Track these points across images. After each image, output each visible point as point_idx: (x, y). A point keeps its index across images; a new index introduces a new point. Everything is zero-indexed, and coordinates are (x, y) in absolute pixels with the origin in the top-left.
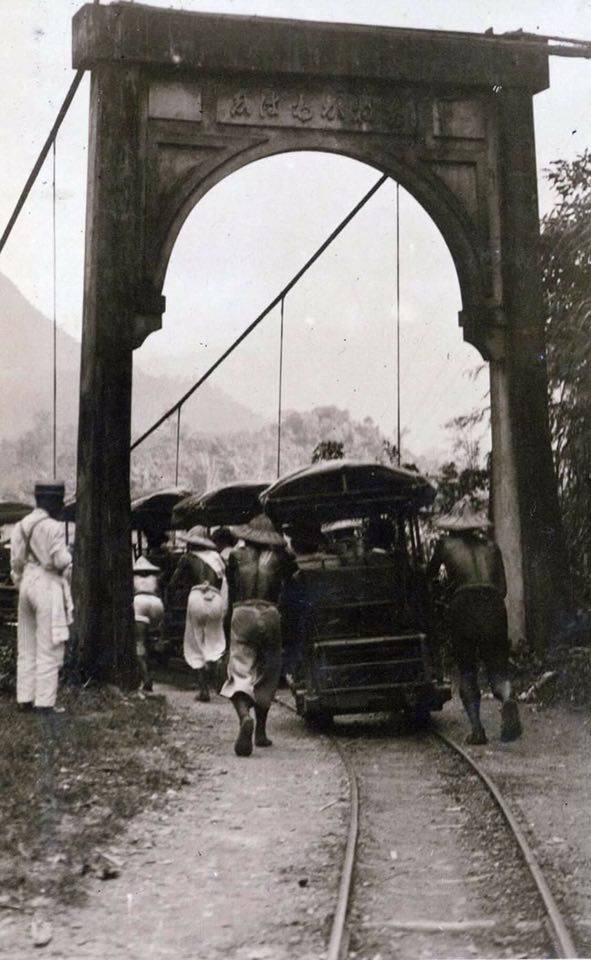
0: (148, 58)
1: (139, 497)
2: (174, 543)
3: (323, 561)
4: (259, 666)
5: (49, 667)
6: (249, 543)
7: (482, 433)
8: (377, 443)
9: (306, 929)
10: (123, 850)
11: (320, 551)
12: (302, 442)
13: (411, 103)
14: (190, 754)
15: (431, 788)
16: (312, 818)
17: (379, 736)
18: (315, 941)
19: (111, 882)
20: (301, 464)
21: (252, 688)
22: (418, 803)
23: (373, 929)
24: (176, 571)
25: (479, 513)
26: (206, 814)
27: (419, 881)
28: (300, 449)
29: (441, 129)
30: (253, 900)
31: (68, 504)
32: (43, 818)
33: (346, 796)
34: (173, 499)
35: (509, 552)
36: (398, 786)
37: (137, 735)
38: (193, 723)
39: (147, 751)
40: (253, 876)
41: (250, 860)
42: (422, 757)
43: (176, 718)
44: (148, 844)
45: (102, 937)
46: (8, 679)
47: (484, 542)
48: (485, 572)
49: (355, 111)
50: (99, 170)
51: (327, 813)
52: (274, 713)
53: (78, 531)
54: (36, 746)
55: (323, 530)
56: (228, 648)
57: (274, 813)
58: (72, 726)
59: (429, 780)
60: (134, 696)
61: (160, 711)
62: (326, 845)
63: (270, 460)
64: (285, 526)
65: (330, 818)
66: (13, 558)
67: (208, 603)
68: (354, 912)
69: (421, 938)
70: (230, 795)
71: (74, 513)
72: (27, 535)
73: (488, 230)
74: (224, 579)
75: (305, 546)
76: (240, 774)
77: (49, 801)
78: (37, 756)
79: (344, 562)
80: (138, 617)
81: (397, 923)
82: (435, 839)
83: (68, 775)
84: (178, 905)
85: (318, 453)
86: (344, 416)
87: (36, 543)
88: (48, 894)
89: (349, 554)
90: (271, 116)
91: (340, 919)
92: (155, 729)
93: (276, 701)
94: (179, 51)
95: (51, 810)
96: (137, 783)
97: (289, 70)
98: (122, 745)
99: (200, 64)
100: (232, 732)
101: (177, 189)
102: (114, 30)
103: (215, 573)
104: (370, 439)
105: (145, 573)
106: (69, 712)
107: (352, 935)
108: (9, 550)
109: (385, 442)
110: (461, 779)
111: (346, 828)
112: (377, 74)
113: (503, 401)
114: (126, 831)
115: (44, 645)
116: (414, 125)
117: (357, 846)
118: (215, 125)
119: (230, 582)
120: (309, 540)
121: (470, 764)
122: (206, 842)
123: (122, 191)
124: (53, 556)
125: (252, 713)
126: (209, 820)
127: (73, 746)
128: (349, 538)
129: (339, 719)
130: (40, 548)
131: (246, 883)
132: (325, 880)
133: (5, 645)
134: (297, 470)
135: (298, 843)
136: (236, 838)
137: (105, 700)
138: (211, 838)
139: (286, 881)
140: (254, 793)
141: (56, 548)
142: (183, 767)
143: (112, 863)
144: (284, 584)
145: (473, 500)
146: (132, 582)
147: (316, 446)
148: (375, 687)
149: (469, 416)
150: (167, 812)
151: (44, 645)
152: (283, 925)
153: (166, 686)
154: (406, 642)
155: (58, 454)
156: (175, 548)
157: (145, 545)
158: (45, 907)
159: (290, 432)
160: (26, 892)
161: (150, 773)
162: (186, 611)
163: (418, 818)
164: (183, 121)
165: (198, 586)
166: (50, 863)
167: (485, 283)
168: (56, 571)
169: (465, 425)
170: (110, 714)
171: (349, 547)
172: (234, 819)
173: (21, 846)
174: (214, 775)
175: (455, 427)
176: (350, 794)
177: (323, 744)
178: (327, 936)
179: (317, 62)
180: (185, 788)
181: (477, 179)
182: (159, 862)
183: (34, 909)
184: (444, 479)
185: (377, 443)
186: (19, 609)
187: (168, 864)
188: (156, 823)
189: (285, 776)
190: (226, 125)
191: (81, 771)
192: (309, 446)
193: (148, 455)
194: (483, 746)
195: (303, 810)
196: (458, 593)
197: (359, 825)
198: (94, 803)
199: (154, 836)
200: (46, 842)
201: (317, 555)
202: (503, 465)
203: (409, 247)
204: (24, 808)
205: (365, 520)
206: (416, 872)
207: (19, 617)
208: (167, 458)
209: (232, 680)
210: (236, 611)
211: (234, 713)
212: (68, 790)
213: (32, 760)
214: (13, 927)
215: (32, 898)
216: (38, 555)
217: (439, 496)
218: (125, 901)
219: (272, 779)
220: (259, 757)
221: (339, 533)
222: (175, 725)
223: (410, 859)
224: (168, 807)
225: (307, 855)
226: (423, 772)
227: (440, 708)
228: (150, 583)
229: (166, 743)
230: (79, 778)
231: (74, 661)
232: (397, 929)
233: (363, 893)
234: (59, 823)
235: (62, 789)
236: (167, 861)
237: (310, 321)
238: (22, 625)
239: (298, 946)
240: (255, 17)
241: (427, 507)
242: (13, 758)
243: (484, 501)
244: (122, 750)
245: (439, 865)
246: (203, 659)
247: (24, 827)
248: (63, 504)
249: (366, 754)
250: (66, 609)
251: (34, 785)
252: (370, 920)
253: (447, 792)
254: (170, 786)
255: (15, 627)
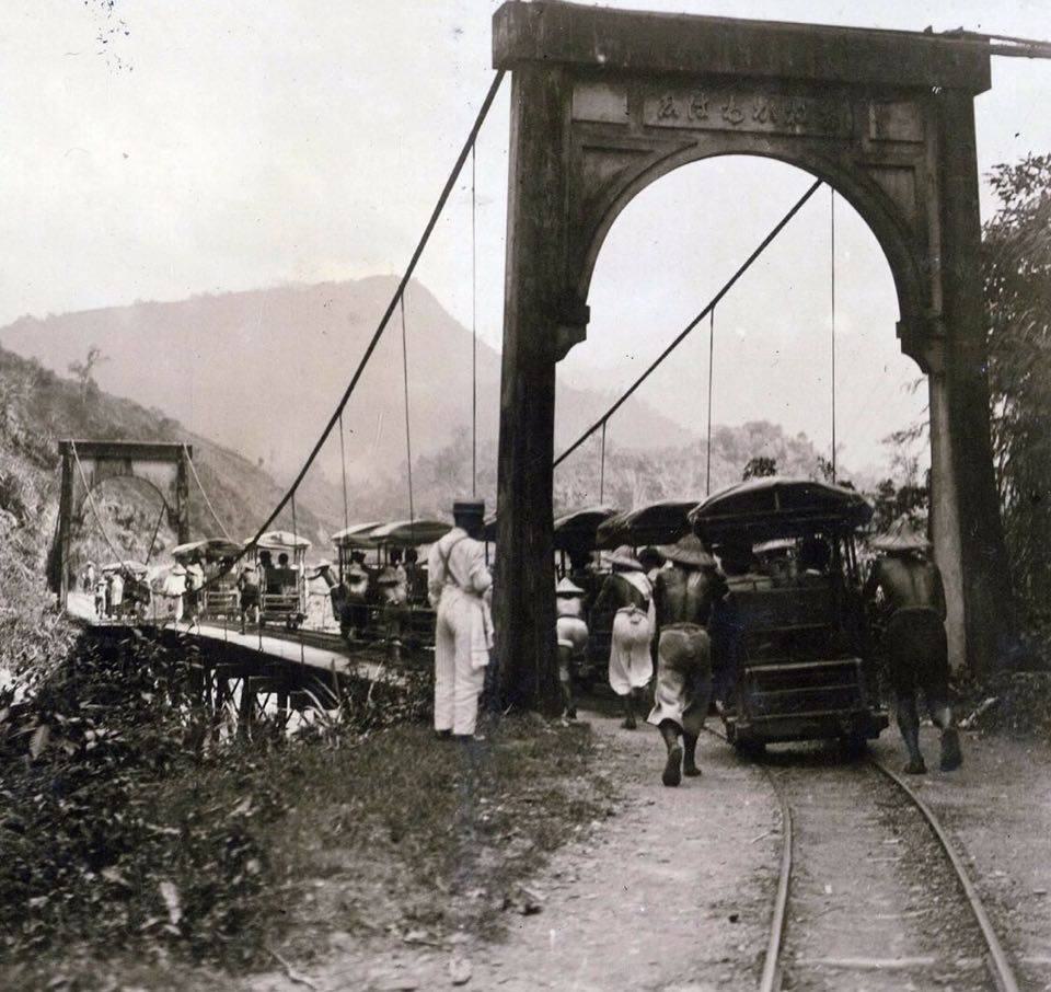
0: (573, 58)
1: (562, 516)
2: (599, 563)
3: (754, 583)
4: (688, 692)
5: (468, 693)
6: (677, 563)
7: (921, 450)
8: (811, 459)
9: (737, 967)
10: (546, 884)
11: (752, 572)
12: (732, 458)
13: (846, 105)
14: (615, 783)
15: (869, 819)
16: (744, 851)
17: (813, 766)
18: (746, 979)
19: (533, 918)
20: (731, 482)
21: (680, 715)
22: (854, 835)
23: (807, 966)
24: (601, 593)
25: (917, 532)
26: (632, 846)
27: (854, 916)
28: (731, 466)
29: (878, 132)
30: (682, 936)
31: (487, 523)
32: (463, 851)
33: (779, 827)
34: (597, 518)
35: (950, 574)
36: (833, 817)
37: (560, 764)
38: (619, 751)
39: (571, 781)
40: (681, 911)
41: (678, 895)
42: (859, 787)
43: (601, 746)
44: (572, 878)
45: (523, 974)
46: (425, 706)
47: (923, 563)
48: (924, 594)
49: (788, 113)
50: (520, 176)
51: (759, 845)
52: (704, 741)
53: (499, 552)
54: (455, 776)
55: (755, 550)
56: (655, 673)
57: (703, 846)
58: (492, 754)
59: (865, 811)
60: (558, 723)
61: (584, 738)
62: (758, 879)
63: (699, 478)
64: (715, 546)
65: (763, 851)
66: (430, 580)
67: (636, 627)
68: (787, 948)
69: (857, 975)
70: (658, 827)
71: (494, 532)
72: (445, 555)
73: (927, 238)
74: (652, 601)
75: (735, 568)
76: (668, 805)
77: (468, 833)
78: (456, 785)
79: (776, 583)
80: (562, 641)
81: (831, 960)
82: (871, 873)
83: (488, 806)
84: (603, 941)
85: (750, 469)
86: (777, 431)
87: (454, 564)
88: (467, 930)
89: (783, 575)
90: (699, 118)
91: (772, 957)
92: (579, 758)
93: (706, 729)
94: (604, 51)
95: (470, 842)
96: (560, 815)
97: (719, 70)
98: (544, 775)
99: (626, 64)
100: (659, 761)
101: (602, 194)
102: (536, 29)
103: (642, 595)
104: (804, 454)
105: (568, 595)
106: (489, 739)
107: (785, 973)
108: (426, 571)
109: (819, 459)
110: (898, 810)
111: (778, 861)
112: (811, 74)
113: (943, 416)
114: (549, 864)
115: (462, 670)
116: (850, 127)
117: (790, 880)
118: (642, 128)
119: (658, 605)
120: (740, 561)
121: (908, 794)
122: (633, 876)
123: (545, 196)
124: (472, 578)
125: (681, 741)
126: (634, 854)
127: (493, 775)
128: (781, 559)
129: (769, 747)
130: (459, 569)
131: (674, 919)
132: (756, 915)
133: (422, 670)
134: (728, 487)
135: (729, 877)
136: (663, 872)
137: (526, 727)
138: (638, 872)
139: (716, 917)
140: (683, 825)
141: (476, 569)
142: (608, 797)
143: (534, 897)
144: (714, 607)
145: (911, 518)
146: (554, 605)
147: (748, 462)
148: (810, 714)
149: (907, 431)
150: (592, 844)
151: (462, 670)
152: (713, 963)
153: (591, 713)
154: (839, 667)
155: (478, 471)
156: (600, 569)
157: (568, 566)
158: (464, 944)
159: (720, 448)
160: (444, 927)
161: (574, 803)
162: (611, 634)
163: (853, 851)
164: (608, 124)
165: (624, 609)
166: (468, 898)
167: (924, 292)
168: (476, 592)
169: (902, 441)
170: (532, 743)
171: (781, 568)
172: (661, 851)
173: (438, 881)
174: (640, 806)
175: (894, 442)
176: (783, 825)
177: (754, 773)
178: (759, 974)
179: (749, 62)
180: (610, 819)
181: (915, 184)
182: (583, 897)
183: (453, 945)
184: (880, 497)
185: (811, 459)
186: (437, 632)
187: (592, 899)
188: (579, 855)
189: (715, 807)
190: (653, 127)
191: (502, 801)
192: (740, 463)
193: (572, 472)
194: (921, 776)
195: (734, 843)
196: (895, 616)
197: (792, 858)
198: (515, 835)
199: (578, 870)
200: (465, 876)
201: (748, 576)
202: (943, 482)
203: (844, 255)
204: (442, 841)
205: (799, 539)
206: (852, 907)
207: (437, 641)
208: (592, 474)
209: (660, 707)
210: (664, 635)
211: (662, 741)
212: (488, 821)
213: (451, 790)
214: (431, 964)
215: (450, 934)
216: (456, 575)
217: (876, 515)
218: (547, 938)
219: (701, 810)
220: (688, 787)
221: (770, 553)
222: (600, 753)
223: (845, 893)
224: (593, 840)
225: (738, 889)
226: (859, 803)
227: (877, 736)
228: (573, 605)
229: (591, 773)
230: (500, 808)
231: (494, 687)
232: (832, 967)
233: (796, 929)
234: (478, 856)
235: (481, 821)
236: (592, 896)
237: (741, 332)
238: (439, 650)
239: (728, 985)
240: (684, 14)
241: (864, 526)
242: (432, 788)
243: (922, 520)
244: (545, 779)
245: (875, 899)
246: (629, 685)
247: (443, 860)
248: (483, 523)
249: (800, 784)
250: (486, 632)
251: (452, 816)
252: (804, 958)
253: (884, 823)
254: (595, 817)
255: (433, 652)
